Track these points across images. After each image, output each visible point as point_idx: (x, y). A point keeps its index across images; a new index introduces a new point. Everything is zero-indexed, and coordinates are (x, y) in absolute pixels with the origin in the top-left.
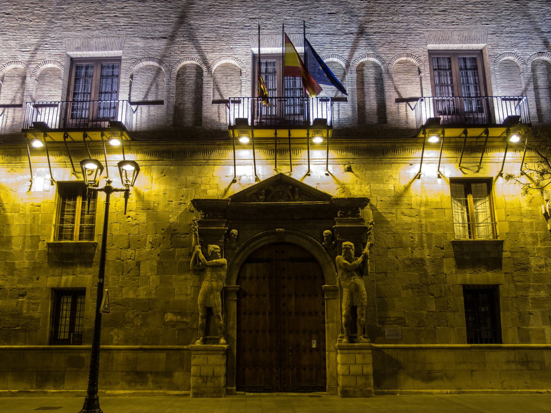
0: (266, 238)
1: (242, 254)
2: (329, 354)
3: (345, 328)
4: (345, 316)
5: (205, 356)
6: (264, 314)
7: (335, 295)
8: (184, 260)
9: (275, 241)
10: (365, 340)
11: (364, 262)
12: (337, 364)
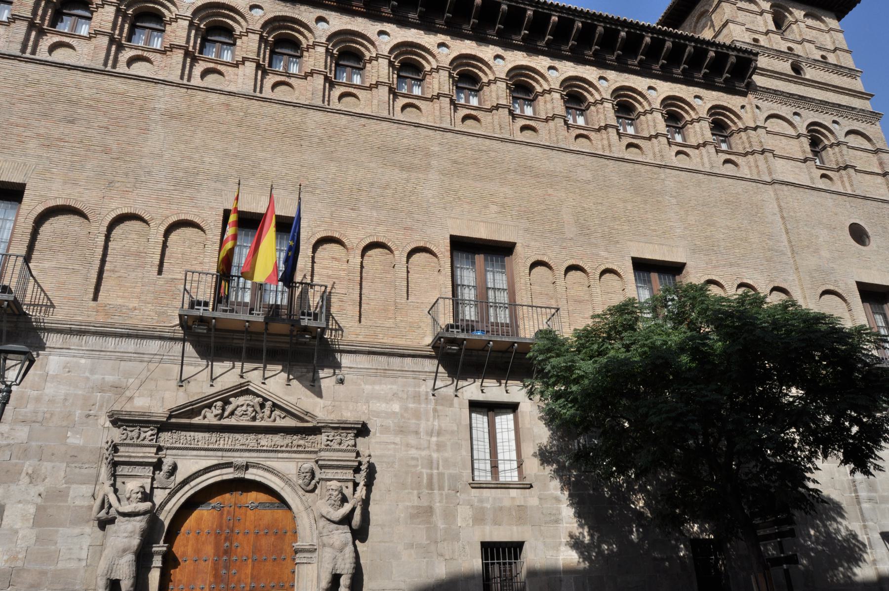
9: (231, 477)
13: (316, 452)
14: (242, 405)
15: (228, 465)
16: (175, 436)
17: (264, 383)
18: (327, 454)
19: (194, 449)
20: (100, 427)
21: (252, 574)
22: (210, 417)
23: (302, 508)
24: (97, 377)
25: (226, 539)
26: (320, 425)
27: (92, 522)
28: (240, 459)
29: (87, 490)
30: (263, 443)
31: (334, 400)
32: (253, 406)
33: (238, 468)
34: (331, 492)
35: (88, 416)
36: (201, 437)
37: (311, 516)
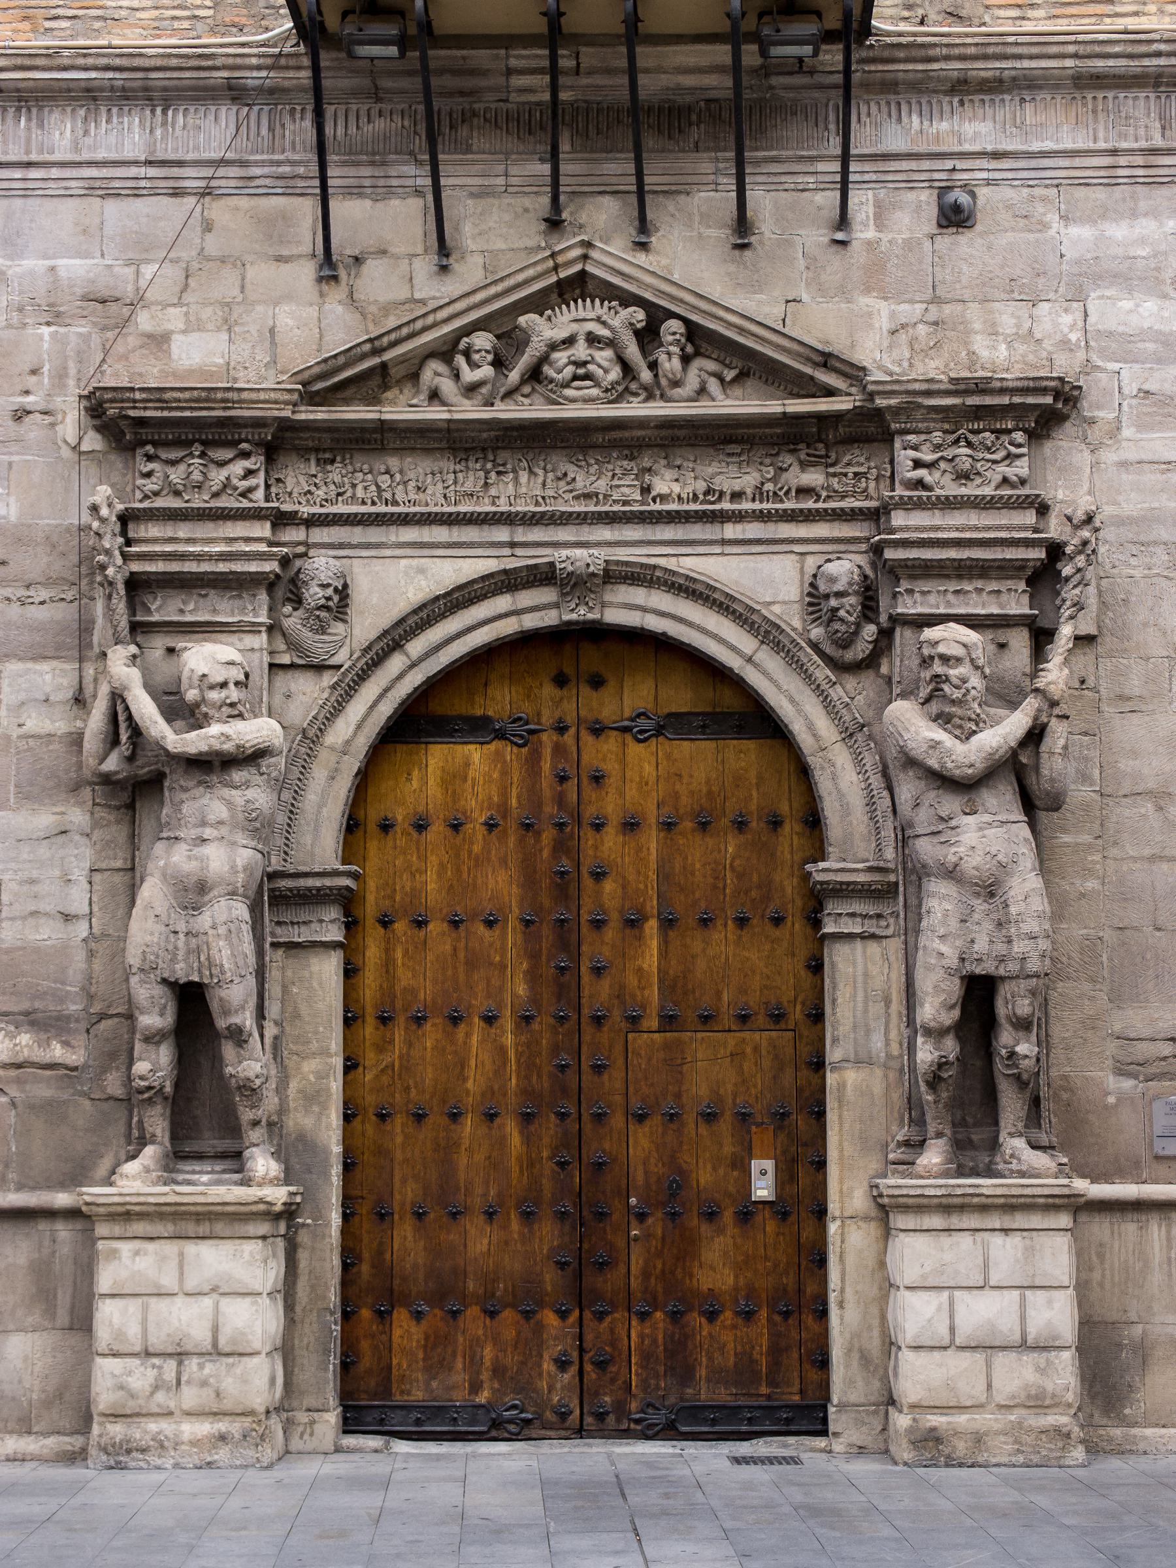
0: (503, 603)
1: (369, 691)
5: (170, 1248)
6: (489, 1020)
7: (879, 916)
8: (47, 726)
9: (549, 619)
10: (1041, 1160)
11: (1035, 736)
13: (877, 515)
14: (570, 341)
15: (542, 576)
16: (336, 473)
17: (643, 246)
18: (918, 518)
19: (405, 520)
20: (66, 453)
22: (455, 398)
23: (826, 728)
24: (33, 264)
25: (560, 847)
26: (880, 402)
27: (87, 792)
28: (580, 552)
29: (53, 677)
30: (661, 486)
31: (936, 300)
32: (611, 343)
33: (575, 584)
34: (938, 668)
35: (20, 415)
36: (426, 484)
37: (870, 759)
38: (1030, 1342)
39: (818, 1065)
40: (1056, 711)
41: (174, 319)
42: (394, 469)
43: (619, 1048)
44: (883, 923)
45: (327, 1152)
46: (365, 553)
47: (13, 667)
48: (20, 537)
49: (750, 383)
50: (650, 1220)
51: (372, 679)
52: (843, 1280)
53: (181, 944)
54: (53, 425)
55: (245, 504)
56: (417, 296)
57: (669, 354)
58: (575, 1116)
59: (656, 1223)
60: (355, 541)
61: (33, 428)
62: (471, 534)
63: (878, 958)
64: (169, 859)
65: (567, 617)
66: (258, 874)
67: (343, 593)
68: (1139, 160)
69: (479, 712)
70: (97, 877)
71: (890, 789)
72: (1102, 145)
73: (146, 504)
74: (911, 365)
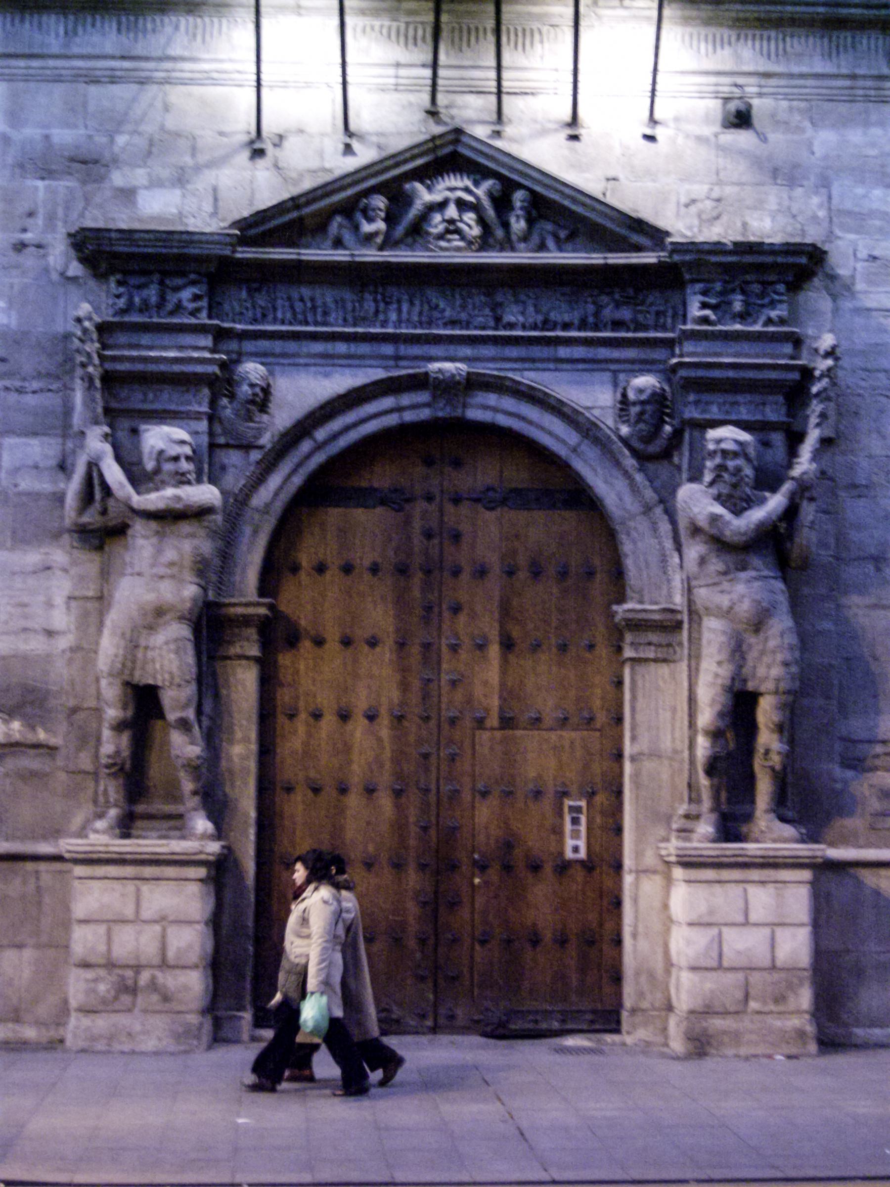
0: (388, 402)
1: (285, 467)
2: (637, 884)
3: (704, 781)
4: (707, 733)
6: (371, 717)
7: (669, 645)
9: (425, 414)
10: (789, 830)
11: (791, 512)
12: (668, 922)
14: (442, 206)
15: (418, 382)
21: (503, 684)
23: (631, 504)
24: (31, 132)
27: (66, 538)
29: (41, 449)
30: (509, 318)
32: (476, 208)
35: (20, 247)
38: (725, 964)
39: (619, 756)
40: (807, 494)
41: (139, 176)
42: (306, 299)
43: (467, 743)
44: (671, 650)
45: (247, 815)
46: (282, 361)
47: (10, 441)
48: (18, 339)
49: (580, 240)
50: (490, 871)
51: (287, 458)
52: (636, 918)
53: (140, 655)
54: (44, 256)
55: (193, 321)
56: (327, 165)
57: (518, 217)
58: (434, 791)
59: (493, 874)
60: (278, 350)
61: (29, 259)
62: (364, 348)
63: (667, 676)
64: (132, 593)
65: (440, 414)
66: (200, 604)
67: (266, 391)
68: (869, 83)
69: (364, 484)
70: (74, 604)
71: (679, 548)
72: (844, 71)
73: (116, 319)
74: (700, 231)
